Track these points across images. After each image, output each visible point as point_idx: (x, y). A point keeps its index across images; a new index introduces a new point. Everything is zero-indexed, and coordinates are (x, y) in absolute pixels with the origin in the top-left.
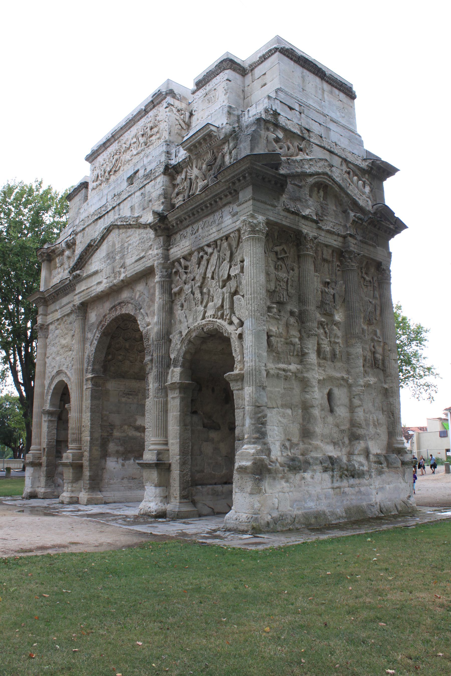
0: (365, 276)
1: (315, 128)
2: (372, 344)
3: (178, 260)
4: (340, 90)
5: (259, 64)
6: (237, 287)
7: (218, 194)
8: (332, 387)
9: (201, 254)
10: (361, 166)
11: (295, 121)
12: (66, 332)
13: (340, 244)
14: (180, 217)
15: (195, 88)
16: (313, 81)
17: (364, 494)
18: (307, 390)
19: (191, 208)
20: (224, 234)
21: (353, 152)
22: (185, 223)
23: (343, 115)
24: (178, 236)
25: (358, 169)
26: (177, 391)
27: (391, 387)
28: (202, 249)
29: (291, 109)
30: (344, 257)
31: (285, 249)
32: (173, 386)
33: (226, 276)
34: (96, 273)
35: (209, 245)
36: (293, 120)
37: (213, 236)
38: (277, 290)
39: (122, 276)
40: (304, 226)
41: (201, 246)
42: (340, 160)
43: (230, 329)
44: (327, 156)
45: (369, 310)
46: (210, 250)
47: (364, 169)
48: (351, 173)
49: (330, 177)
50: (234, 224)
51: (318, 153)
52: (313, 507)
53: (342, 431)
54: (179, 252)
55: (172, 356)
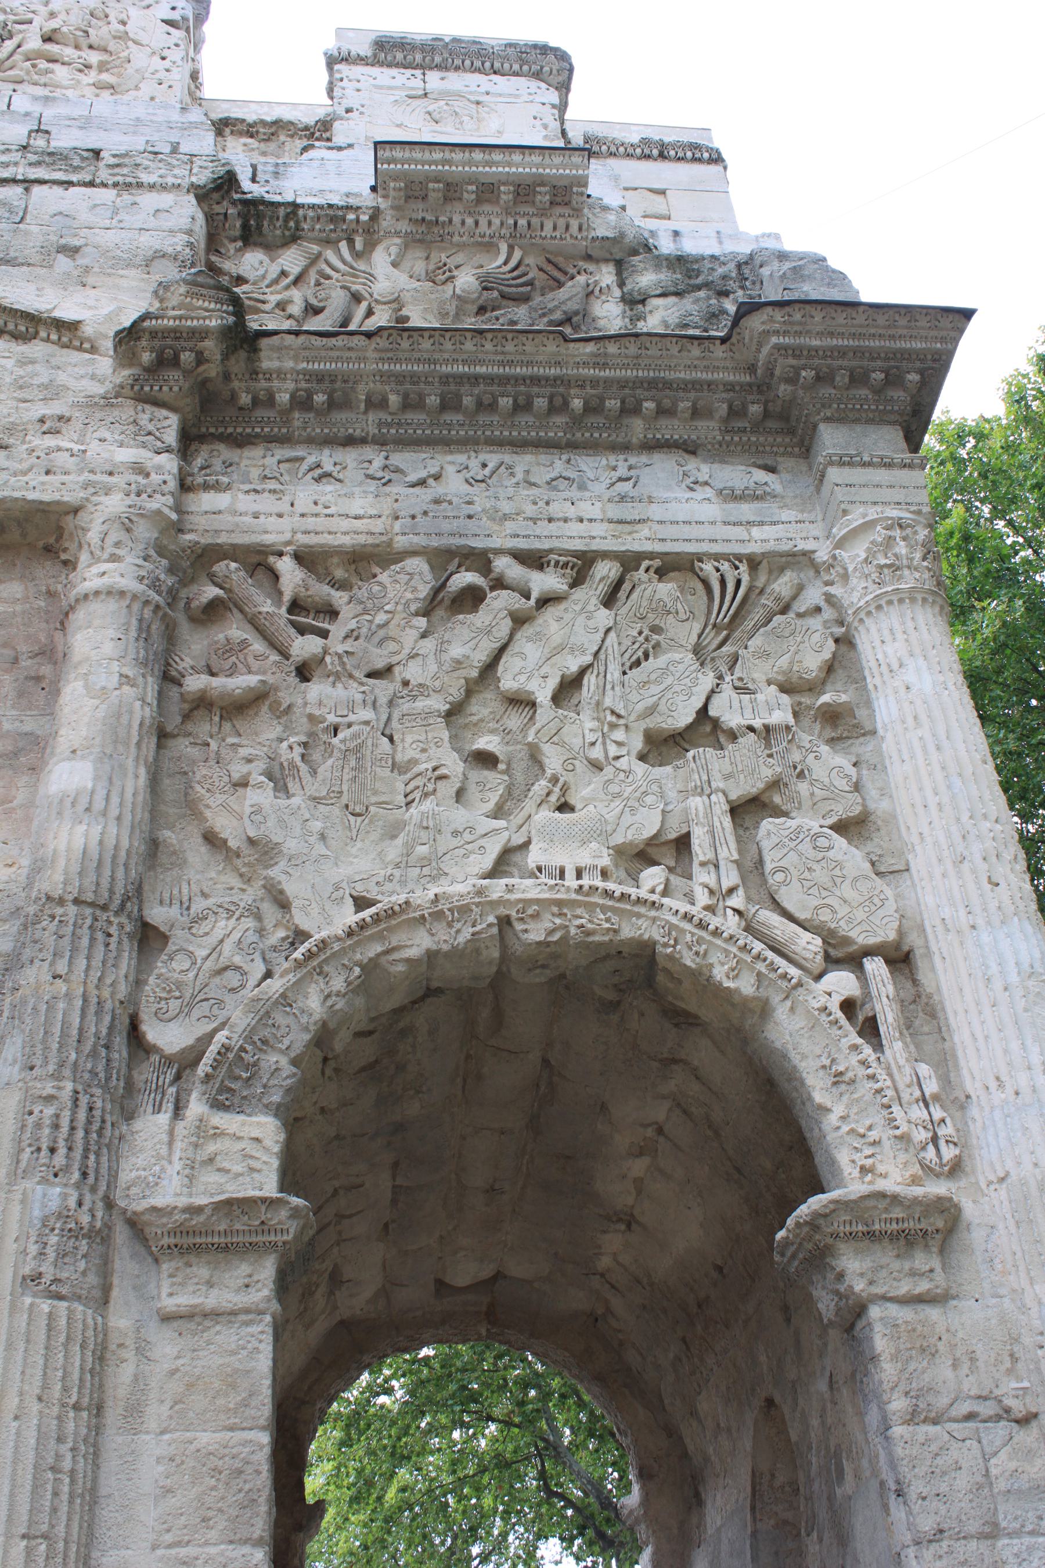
5: (629, 156)
6: (775, 784)
7: (668, 385)
14: (350, 380)
15: (365, 50)
19: (461, 369)
20: (659, 547)
22: (346, 421)
24: (256, 461)
26: (267, 1270)
28: (480, 560)
32: (202, 1238)
33: (684, 717)
35: (534, 560)
37: (574, 528)
41: (478, 544)
50: (739, 532)
54: (286, 524)
55: (168, 1036)
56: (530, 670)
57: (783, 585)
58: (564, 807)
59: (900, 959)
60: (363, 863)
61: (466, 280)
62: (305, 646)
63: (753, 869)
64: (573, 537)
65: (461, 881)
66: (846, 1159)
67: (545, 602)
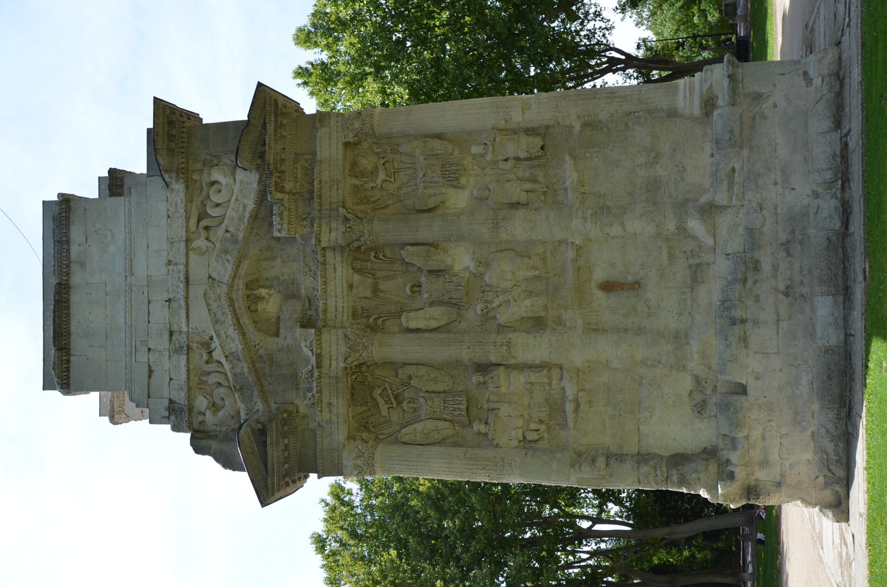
0: (379, 181)
1: (160, 315)
2: (502, 165)
4: (68, 242)
8: (593, 285)
10: (182, 195)
11: (167, 364)
13: (339, 258)
16: (83, 314)
17: (793, 232)
18: (605, 362)
21: (166, 217)
23: (109, 234)
25: (191, 202)
27: (579, 117)
29: (151, 372)
30: (359, 247)
31: (379, 391)
36: (167, 368)
38: (448, 418)
40: (334, 364)
42: (192, 254)
44: (196, 292)
45: (440, 180)
47: (187, 188)
48: (204, 223)
49: (231, 286)
51: (201, 318)
52: (810, 378)
53: (671, 257)
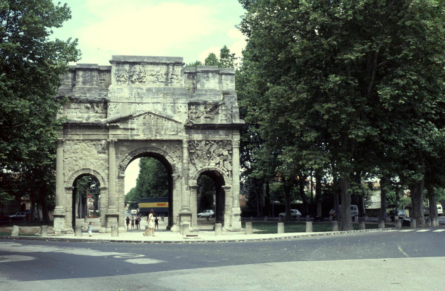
3: (194, 141)
9: (207, 142)
12: (89, 148)
28: (209, 141)
33: (221, 154)
34: (132, 129)
39: (158, 138)
43: (224, 172)
46: (213, 143)
55: (190, 176)
56: (212, 150)
57: (229, 142)
58: (213, 160)
59: (231, 171)
60: (201, 165)
61: (208, 109)
62: (197, 148)
63: (224, 165)
64: (215, 139)
65: (206, 167)
66: (226, 184)
67: (213, 144)
